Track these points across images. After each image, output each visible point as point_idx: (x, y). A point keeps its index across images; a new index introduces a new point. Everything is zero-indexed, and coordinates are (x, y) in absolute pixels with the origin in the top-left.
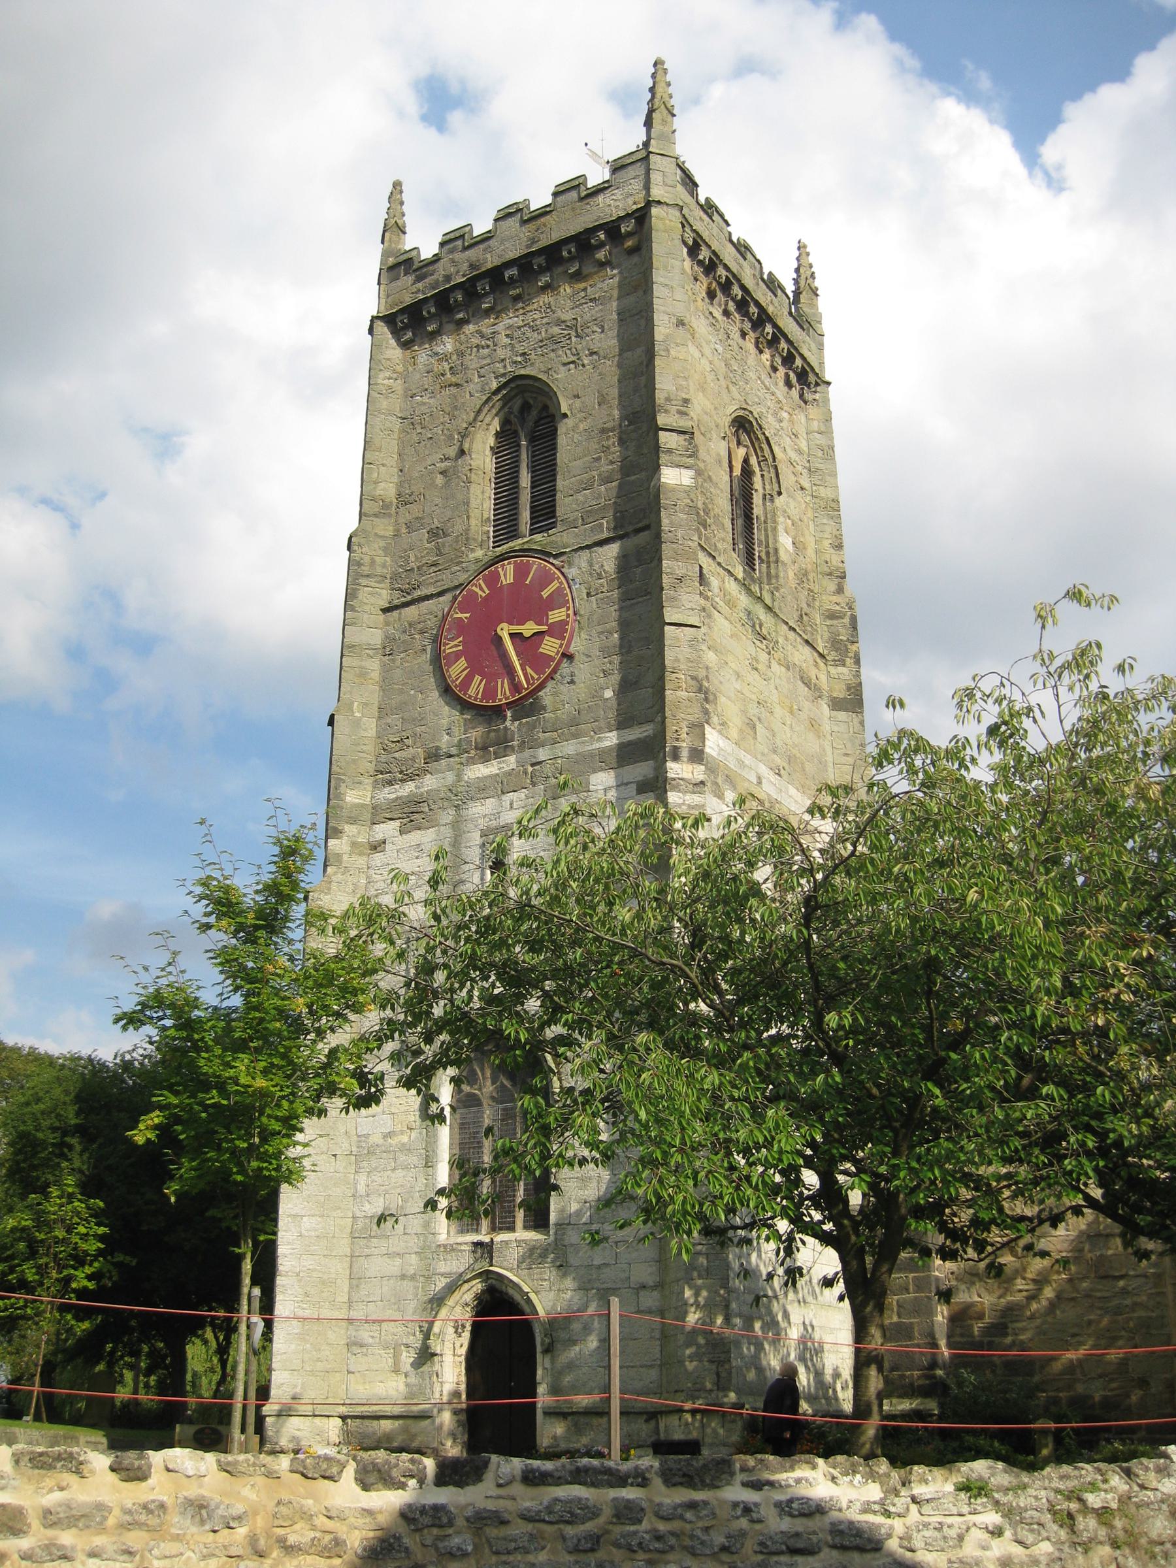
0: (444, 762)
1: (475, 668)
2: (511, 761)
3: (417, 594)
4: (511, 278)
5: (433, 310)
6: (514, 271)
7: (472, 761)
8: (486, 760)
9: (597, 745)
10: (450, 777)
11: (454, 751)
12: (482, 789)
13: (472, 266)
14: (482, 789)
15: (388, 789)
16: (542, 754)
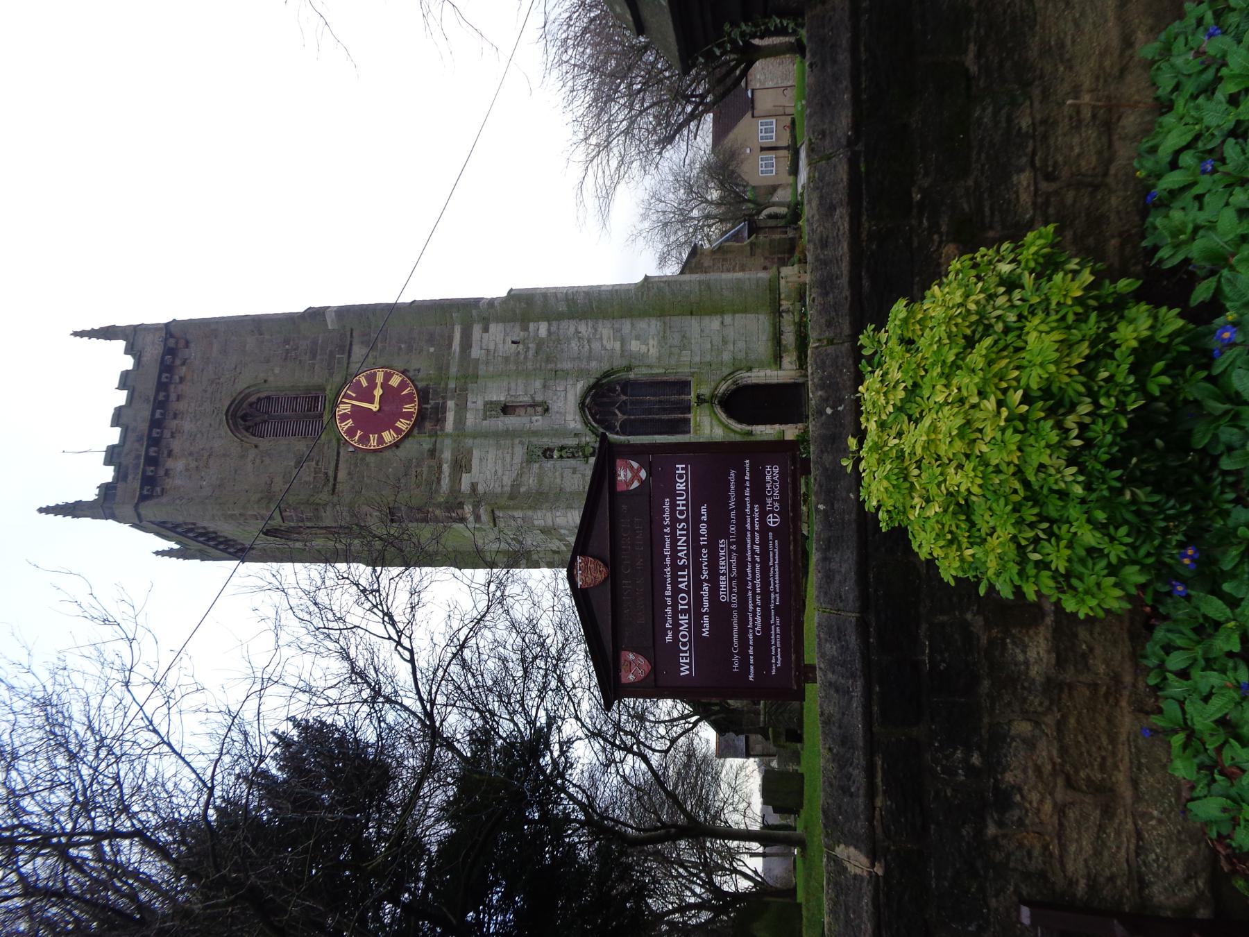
0: (438, 446)
1: (390, 425)
2: (450, 404)
3: (331, 474)
4: (162, 414)
5: (152, 468)
6: (158, 411)
7: (442, 429)
8: (444, 419)
9: (457, 355)
10: (448, 442)
11: (433, 439)
12: (460, 421)
13: (140, 440)
14: (460, 421)
15: (442, 482)
16: (452, 385)
